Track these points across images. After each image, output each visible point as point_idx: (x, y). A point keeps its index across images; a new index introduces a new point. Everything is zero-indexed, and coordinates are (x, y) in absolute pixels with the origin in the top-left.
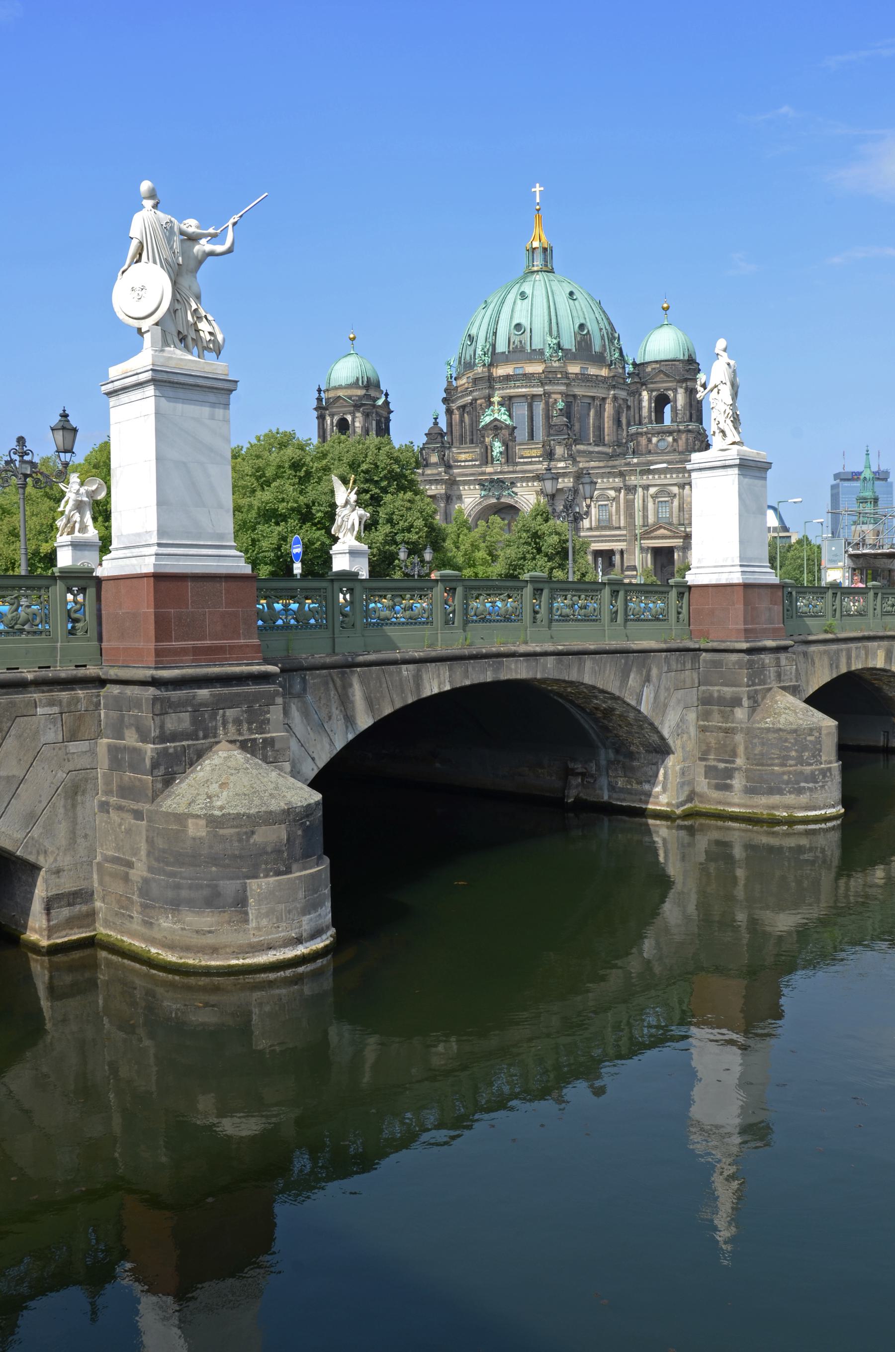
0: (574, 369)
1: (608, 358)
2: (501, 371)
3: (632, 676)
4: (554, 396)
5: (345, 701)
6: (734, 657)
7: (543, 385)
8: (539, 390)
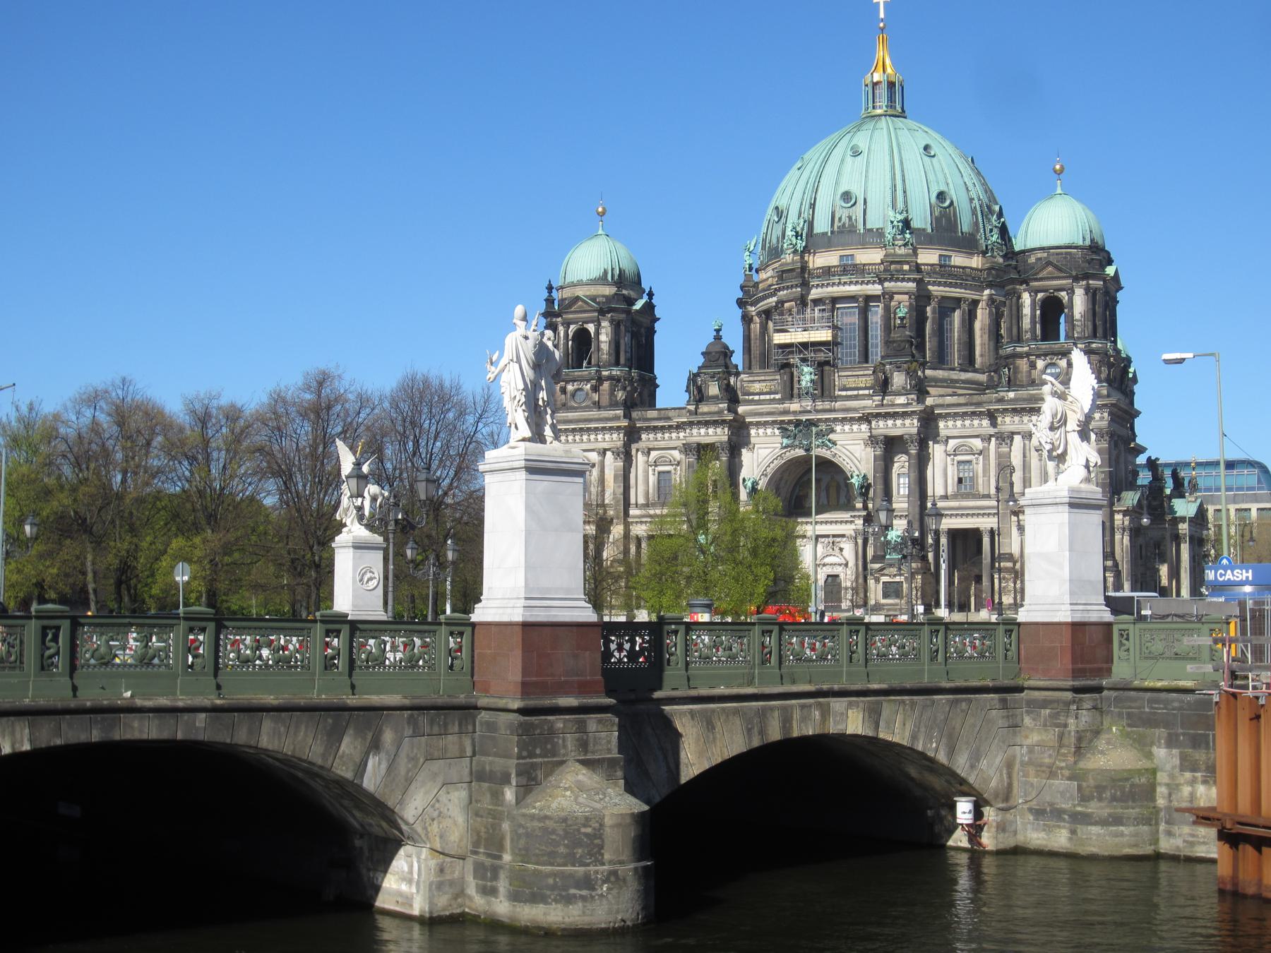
0: (928, 257)
1: (982, 241)
2: (819, 260)
3: (346, 740)
4: (896, 297)
6: (504, 717)
7: (881, 282)
8: (876, 289)
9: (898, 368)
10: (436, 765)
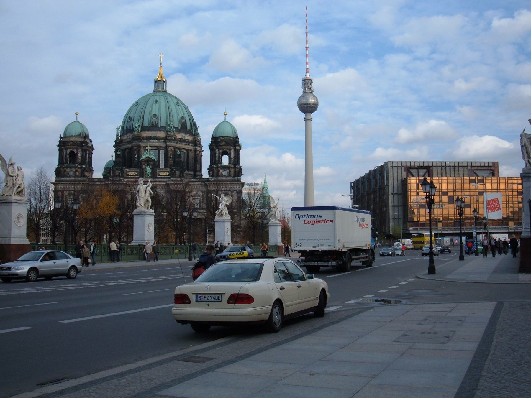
0: (179, 136)
9: (177, 169)
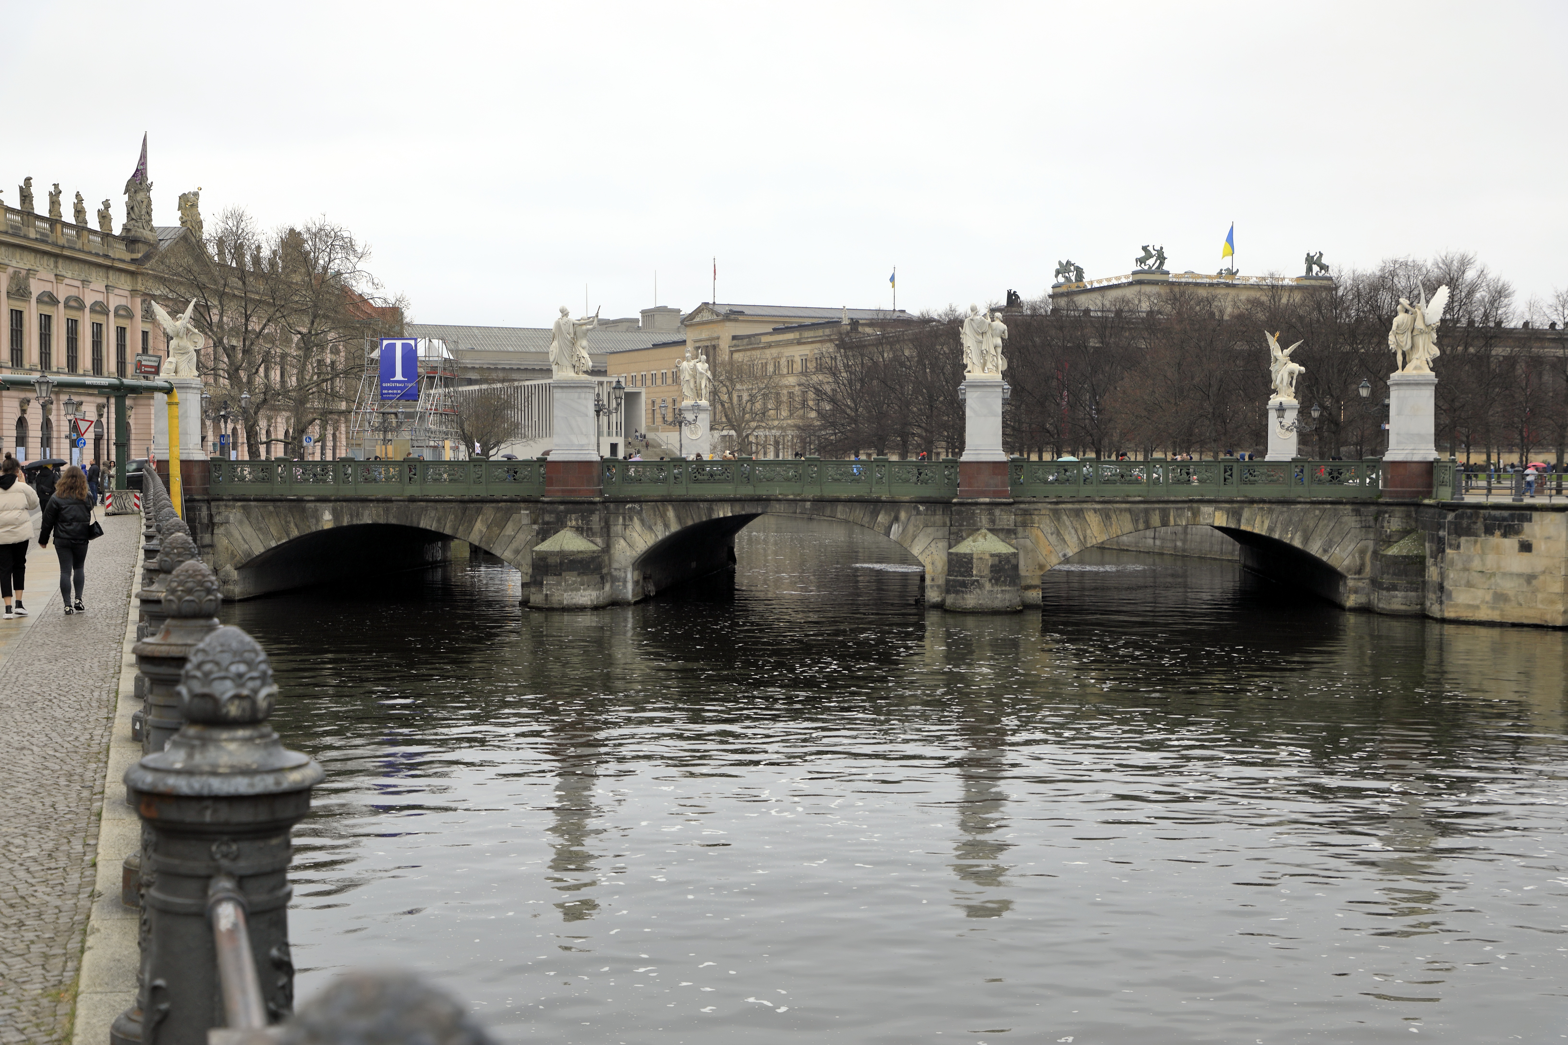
5: (663, 516)
10: (930, 530)
